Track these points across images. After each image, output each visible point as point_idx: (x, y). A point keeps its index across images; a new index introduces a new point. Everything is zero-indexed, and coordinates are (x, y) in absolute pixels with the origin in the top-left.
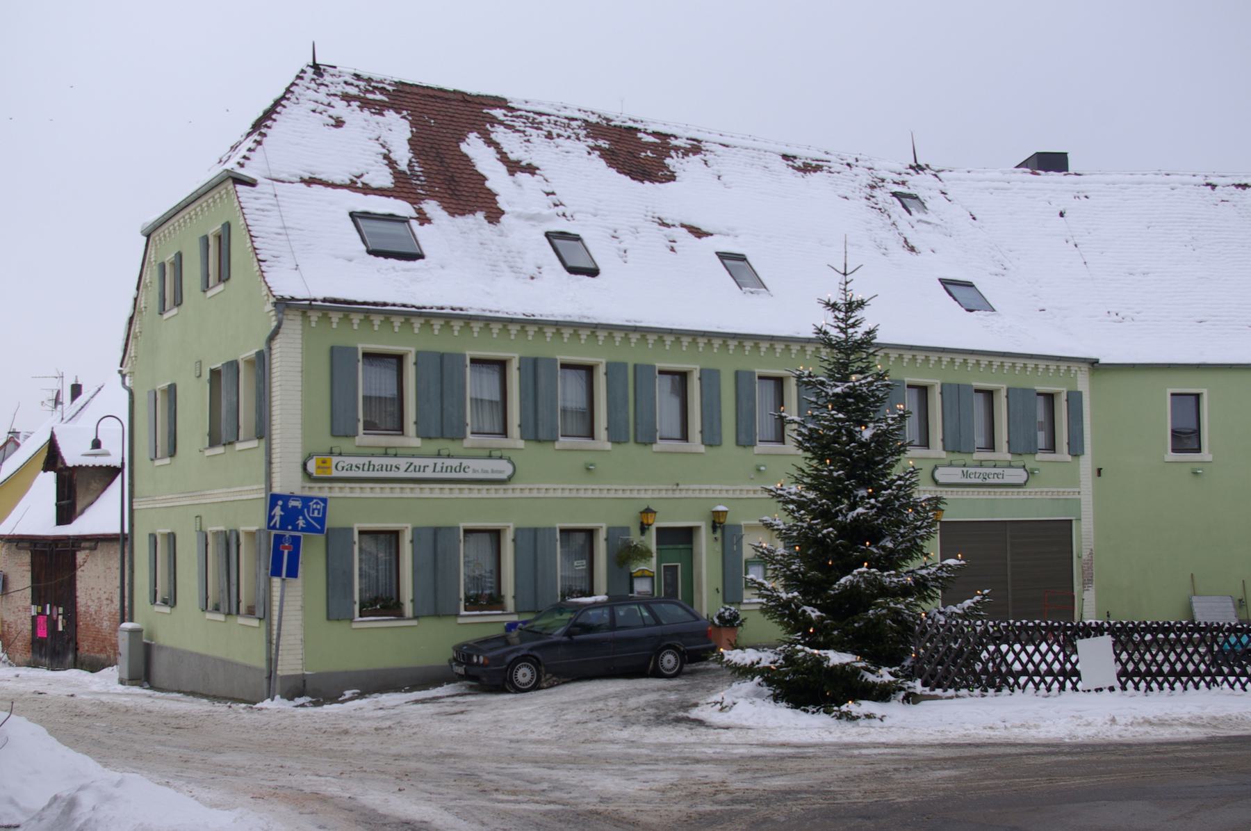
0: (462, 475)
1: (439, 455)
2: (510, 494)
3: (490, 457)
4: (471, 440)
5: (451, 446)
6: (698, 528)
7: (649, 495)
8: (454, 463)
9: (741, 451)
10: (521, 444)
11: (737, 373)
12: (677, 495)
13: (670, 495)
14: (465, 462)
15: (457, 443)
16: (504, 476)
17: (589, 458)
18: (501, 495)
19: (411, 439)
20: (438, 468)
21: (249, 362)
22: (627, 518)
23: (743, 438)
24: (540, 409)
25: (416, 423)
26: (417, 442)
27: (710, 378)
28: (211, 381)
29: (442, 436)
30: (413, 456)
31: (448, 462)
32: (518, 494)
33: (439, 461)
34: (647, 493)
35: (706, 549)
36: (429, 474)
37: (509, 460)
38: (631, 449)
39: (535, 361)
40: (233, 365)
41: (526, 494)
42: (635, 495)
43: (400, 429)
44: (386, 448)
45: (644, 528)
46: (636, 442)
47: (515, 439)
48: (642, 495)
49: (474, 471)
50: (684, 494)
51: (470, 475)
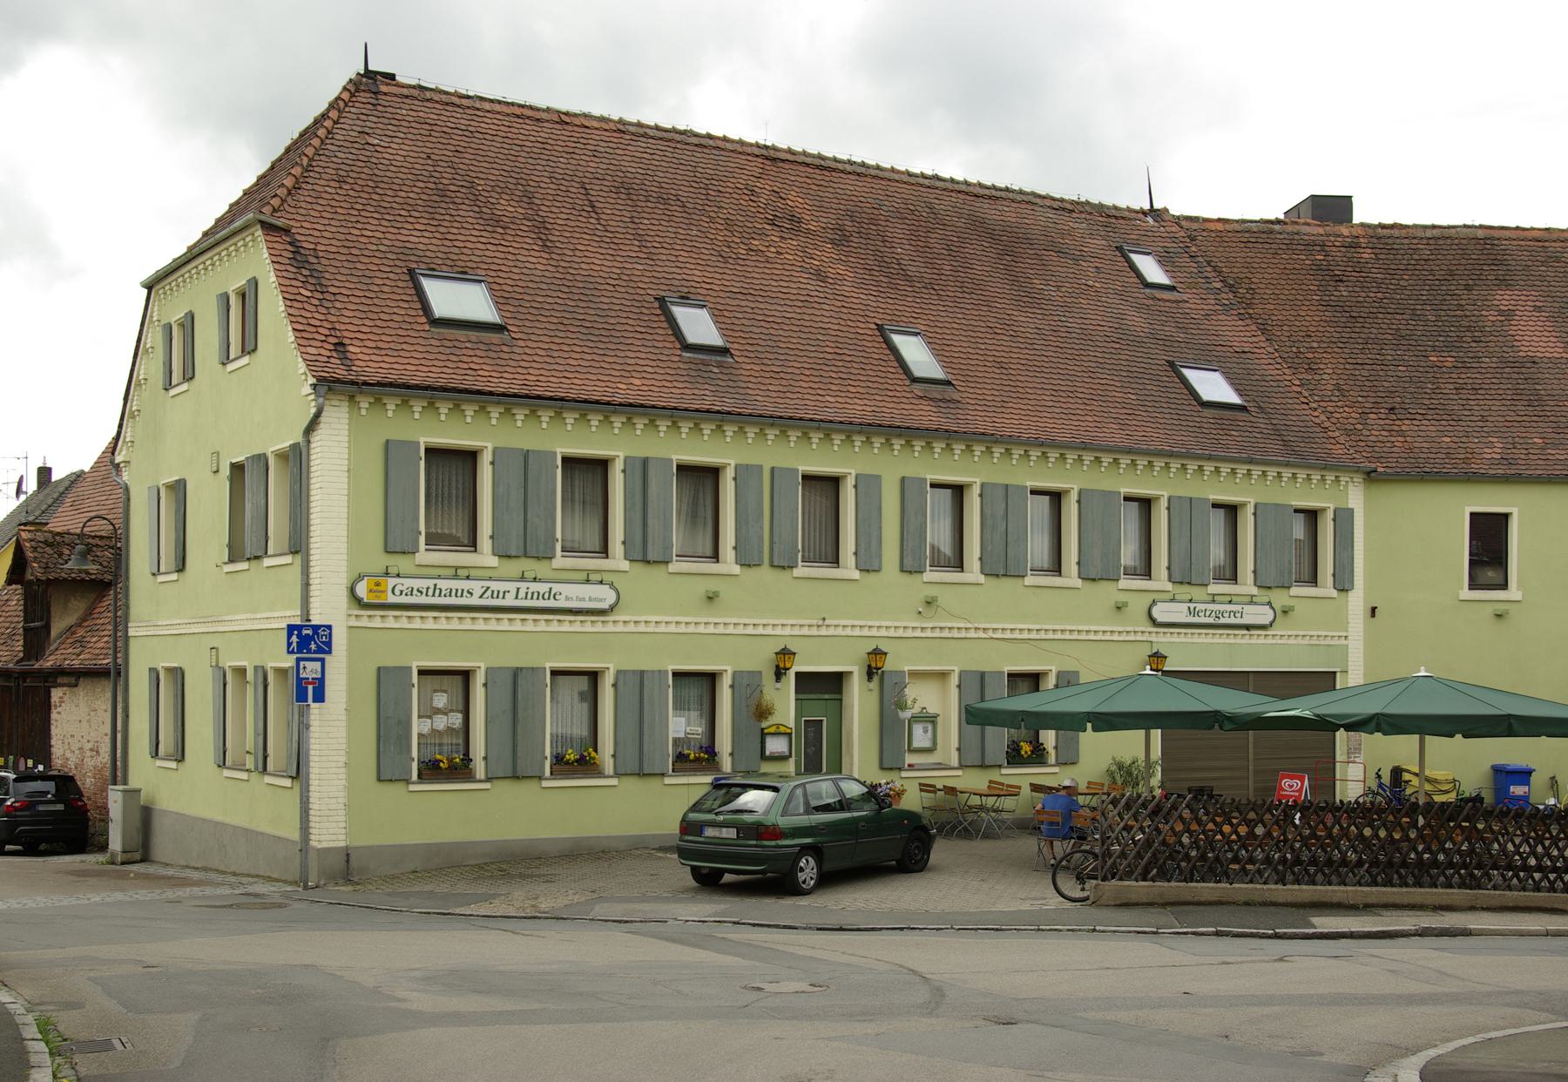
0: (551, 604)
1: (523, 579)
2: (610, 628)
3: (588, 581)
4: (560, 561)
5: (540, 568)
6: (851, 673)
7: (787, 631)
8: (543, 588)
9: (906, 577)
10: (625, 565)
11: (903, 480)
12: (823, 632)
13: (814, 632)
14: (556, 588)
15: (545, 563)
16: (605, 605)
17: (713, 584)
18: (599, 628)
19: (485, 557)
20: (522, 594)
21: (282, 456)
22: (760, 659)
23: (908, 562)
24: (650, 522)
25: (492, 537)
26: (494, 561)
27: (869, 486)
28: (232, 479)
29: (526, 555)
30: (490, 579)
31: (534, 587)
32: (620, 628)
33: (523, 586)
34: (784, 628)
35: (860, 701)
36: (509, 601)
37: (611, 585)
38: (765, 573)
39: (645, 462)
40: (261, 459)
41: (631, 628)
42: (769, 631)
43: (473, 544)
44: (457, 568)
45: (779, 673)
46: (772, 566)
47: (618, 559)
48: (778, 631)
49: (567, 598)
50: (831, 631)
51: (561, 603)
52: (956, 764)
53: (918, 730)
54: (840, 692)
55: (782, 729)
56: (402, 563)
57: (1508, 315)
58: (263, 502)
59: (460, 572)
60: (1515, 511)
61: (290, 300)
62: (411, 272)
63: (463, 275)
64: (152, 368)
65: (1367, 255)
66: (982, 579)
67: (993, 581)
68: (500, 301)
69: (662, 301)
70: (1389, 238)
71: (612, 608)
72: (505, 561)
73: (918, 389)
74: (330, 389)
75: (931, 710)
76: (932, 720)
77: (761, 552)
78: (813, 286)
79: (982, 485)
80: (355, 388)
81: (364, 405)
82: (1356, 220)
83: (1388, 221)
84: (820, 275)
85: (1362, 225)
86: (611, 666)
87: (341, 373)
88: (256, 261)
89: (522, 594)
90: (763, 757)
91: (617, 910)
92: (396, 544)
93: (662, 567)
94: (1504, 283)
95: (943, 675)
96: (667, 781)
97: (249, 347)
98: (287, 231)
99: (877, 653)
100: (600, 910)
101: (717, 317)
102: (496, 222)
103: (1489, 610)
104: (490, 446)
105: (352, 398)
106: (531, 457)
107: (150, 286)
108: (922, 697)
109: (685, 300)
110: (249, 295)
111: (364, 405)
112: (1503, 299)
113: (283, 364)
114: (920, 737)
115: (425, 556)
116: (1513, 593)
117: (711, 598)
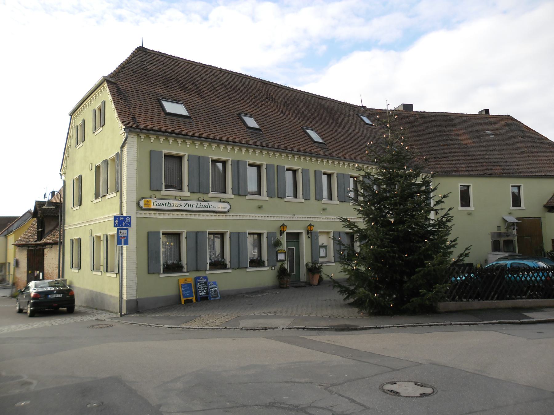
0: (208, 209)
1: (199, 200)
2: (228, 218)
3: (220, 201)
4: (211, 194)
5: (205, 196)
6: (302, 233)
7: (283, 219)
8: (206, 204)
9: (317, 202)
10: (232, 196)
11: (315, 171)
12: (294, 219)
13: (291, 219)
14: (210, 204)
15: (206, 195)
16: (226, 210)
17: (260, 203)
18: (224, 218)
19: (186, 193)
20: (198, 206)
21: (113, 160)
22: (274, 228)
23: (318, 197)
24: (240, 182)
25: (188, 186)
26: (188, 194)
27: (305, 172)
28: (96, 171)
29: (199, 192)
30: (188, 200)
31: (203, 203)
32: (231, 218)
33: (199, 203)
34: (282, 218)
35: (305, 240)
36: (194, 208)
37: (228, 203)
38: (276, 200)
39: (238, 161)
40: (106, 162)
41: (235, 218)
42: (278, 219)
43: (181, 189)
44: (176, 196)
45: (281, 233)
46: (278, 197)
47: (230, 194)
48: (281, 219)
49: (214, 207)
50: (296, 219)
51: (212, 209)
52: (333, 261)
53: (322, 250)
54: (299, 239)
55: (283, 251)
56: (157, 194)
57: (457, 134)
58: (106, 176)
59: (177, 198)
60: (471, 185)
61: (116, 103)
62: (158, 99)
63: (176, 101)
64: (73, 141)
65: (419, 119)
66: (338, 203)
67: (341, 203)
68: (188, 110)
69: (239, 115)
70: (424, 116)
71: (229, 211)
72: (192, 194)
73: (316, 144)
74: (130, 131)
75: (325, 244)
76: (325, 247)
77: (275, 193)
78: (281, 115)
79: (337, 174)
80: (139, 131)
81: (143, 137)
82: (414, 110)
83: (422, 111)
84: (283, 113)
85: (416, 112)
86: (229, 231)
87: (134, 125)
88: (106, 95)
89: (198, 206)
90: (277, 261)
91: (250, 323)
92: (154, 187)
93: (244, 197)
94: (455, 126)
95: (328, 233)
96: (248, 270)
97: (102, 124)
98: (115, 84)
99: (310, 225)
100: (244, 323)
101: (256, 120)
102: (184, 89)
103: (466, 212)
104: (187, 154)
105: (138, 135)
106: (201, 158)
107: (71, 115)
108: (322, 240)
109: (246, 115)
110: (102, 110)
111: (143, 137)
112: (454, 130)
113: (115, 125)
114: (322, 253)
115: (164, 192)
116: (472, 207)
117: (260, 207)
